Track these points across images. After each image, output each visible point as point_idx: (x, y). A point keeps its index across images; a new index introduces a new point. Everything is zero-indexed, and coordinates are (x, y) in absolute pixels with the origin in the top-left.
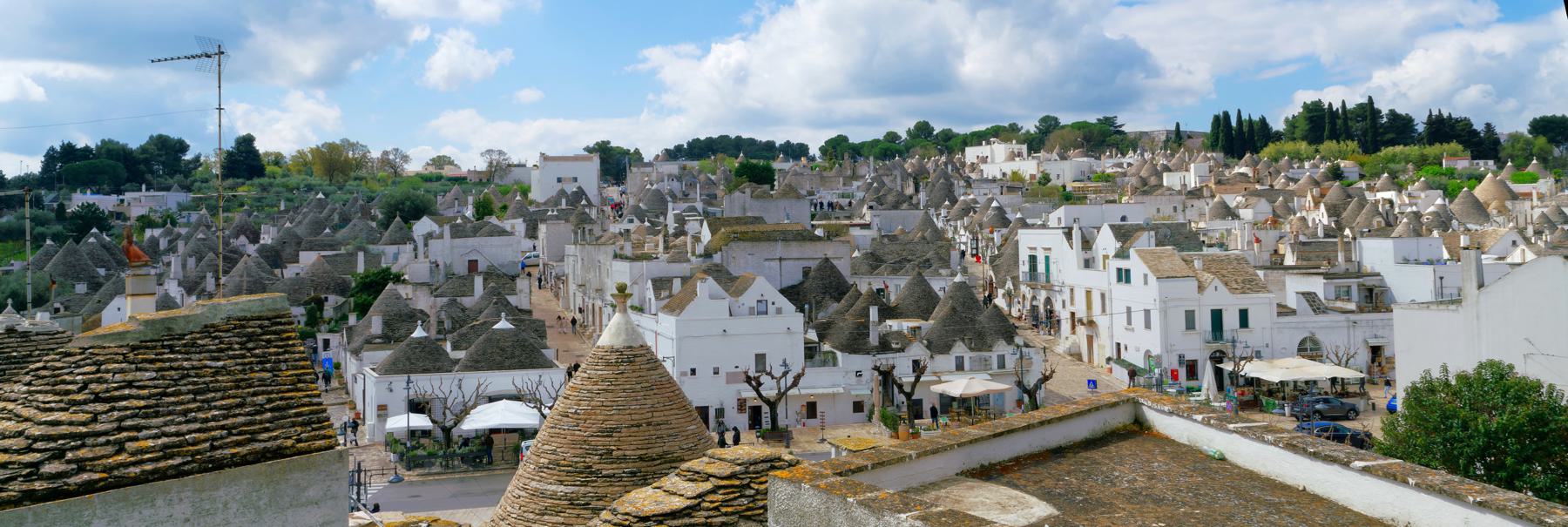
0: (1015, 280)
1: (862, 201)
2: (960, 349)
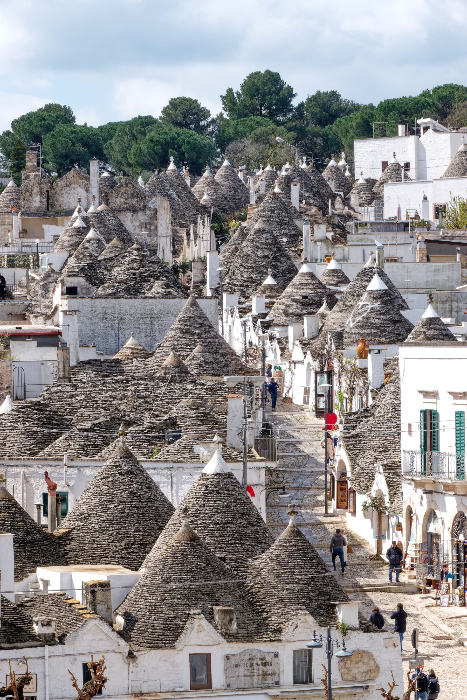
0: (392, 469)
1: (54, 275)
2: (200, 635)
